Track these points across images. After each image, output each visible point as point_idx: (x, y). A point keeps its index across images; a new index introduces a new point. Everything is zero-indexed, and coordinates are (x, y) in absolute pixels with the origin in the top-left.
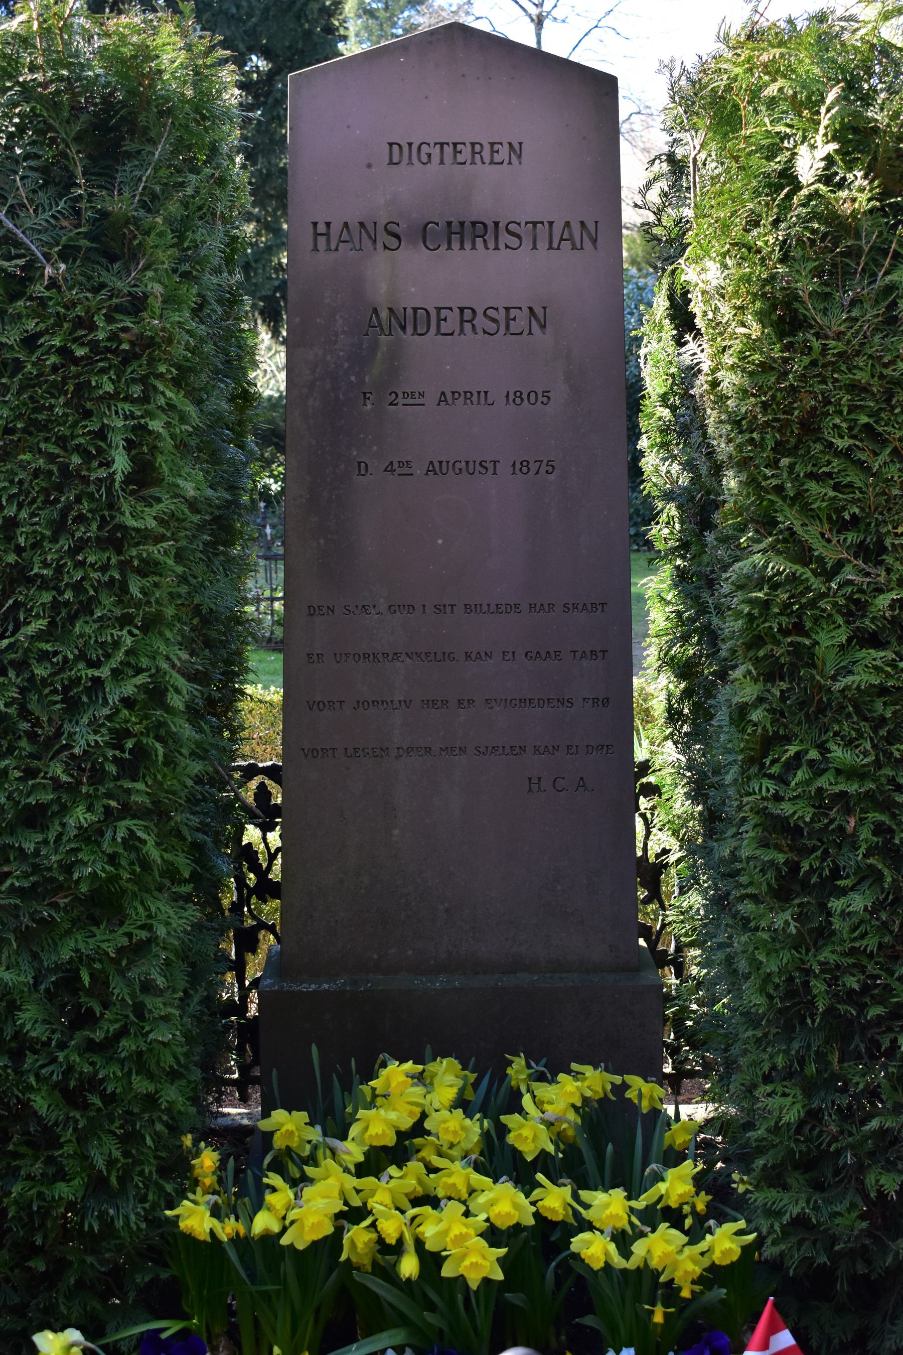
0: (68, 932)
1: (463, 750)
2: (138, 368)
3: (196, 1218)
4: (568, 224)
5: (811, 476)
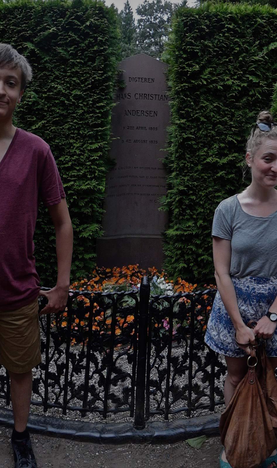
1: (138, 194)
4: (162, 95)
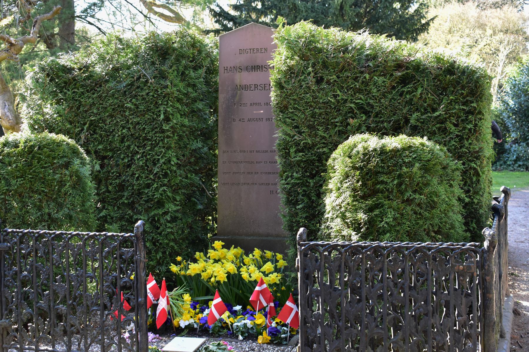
0: (154, 210)
2: (166, 99)
3: (174, 268)
5: (287, 117)
